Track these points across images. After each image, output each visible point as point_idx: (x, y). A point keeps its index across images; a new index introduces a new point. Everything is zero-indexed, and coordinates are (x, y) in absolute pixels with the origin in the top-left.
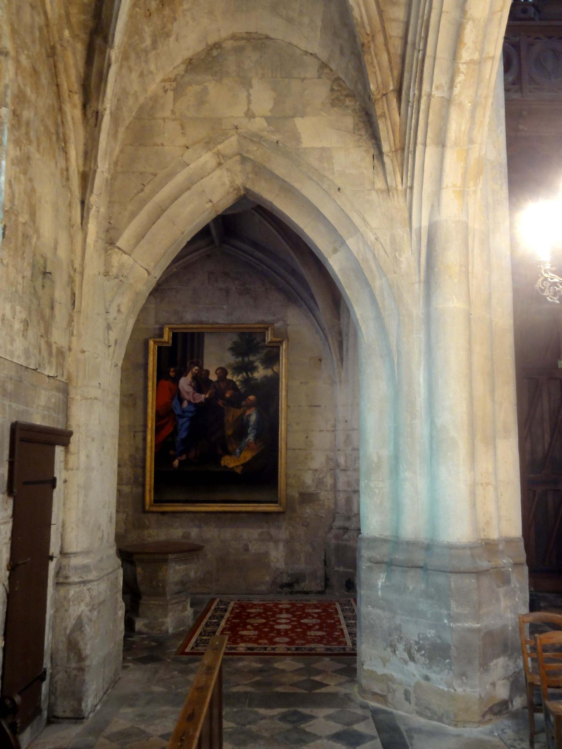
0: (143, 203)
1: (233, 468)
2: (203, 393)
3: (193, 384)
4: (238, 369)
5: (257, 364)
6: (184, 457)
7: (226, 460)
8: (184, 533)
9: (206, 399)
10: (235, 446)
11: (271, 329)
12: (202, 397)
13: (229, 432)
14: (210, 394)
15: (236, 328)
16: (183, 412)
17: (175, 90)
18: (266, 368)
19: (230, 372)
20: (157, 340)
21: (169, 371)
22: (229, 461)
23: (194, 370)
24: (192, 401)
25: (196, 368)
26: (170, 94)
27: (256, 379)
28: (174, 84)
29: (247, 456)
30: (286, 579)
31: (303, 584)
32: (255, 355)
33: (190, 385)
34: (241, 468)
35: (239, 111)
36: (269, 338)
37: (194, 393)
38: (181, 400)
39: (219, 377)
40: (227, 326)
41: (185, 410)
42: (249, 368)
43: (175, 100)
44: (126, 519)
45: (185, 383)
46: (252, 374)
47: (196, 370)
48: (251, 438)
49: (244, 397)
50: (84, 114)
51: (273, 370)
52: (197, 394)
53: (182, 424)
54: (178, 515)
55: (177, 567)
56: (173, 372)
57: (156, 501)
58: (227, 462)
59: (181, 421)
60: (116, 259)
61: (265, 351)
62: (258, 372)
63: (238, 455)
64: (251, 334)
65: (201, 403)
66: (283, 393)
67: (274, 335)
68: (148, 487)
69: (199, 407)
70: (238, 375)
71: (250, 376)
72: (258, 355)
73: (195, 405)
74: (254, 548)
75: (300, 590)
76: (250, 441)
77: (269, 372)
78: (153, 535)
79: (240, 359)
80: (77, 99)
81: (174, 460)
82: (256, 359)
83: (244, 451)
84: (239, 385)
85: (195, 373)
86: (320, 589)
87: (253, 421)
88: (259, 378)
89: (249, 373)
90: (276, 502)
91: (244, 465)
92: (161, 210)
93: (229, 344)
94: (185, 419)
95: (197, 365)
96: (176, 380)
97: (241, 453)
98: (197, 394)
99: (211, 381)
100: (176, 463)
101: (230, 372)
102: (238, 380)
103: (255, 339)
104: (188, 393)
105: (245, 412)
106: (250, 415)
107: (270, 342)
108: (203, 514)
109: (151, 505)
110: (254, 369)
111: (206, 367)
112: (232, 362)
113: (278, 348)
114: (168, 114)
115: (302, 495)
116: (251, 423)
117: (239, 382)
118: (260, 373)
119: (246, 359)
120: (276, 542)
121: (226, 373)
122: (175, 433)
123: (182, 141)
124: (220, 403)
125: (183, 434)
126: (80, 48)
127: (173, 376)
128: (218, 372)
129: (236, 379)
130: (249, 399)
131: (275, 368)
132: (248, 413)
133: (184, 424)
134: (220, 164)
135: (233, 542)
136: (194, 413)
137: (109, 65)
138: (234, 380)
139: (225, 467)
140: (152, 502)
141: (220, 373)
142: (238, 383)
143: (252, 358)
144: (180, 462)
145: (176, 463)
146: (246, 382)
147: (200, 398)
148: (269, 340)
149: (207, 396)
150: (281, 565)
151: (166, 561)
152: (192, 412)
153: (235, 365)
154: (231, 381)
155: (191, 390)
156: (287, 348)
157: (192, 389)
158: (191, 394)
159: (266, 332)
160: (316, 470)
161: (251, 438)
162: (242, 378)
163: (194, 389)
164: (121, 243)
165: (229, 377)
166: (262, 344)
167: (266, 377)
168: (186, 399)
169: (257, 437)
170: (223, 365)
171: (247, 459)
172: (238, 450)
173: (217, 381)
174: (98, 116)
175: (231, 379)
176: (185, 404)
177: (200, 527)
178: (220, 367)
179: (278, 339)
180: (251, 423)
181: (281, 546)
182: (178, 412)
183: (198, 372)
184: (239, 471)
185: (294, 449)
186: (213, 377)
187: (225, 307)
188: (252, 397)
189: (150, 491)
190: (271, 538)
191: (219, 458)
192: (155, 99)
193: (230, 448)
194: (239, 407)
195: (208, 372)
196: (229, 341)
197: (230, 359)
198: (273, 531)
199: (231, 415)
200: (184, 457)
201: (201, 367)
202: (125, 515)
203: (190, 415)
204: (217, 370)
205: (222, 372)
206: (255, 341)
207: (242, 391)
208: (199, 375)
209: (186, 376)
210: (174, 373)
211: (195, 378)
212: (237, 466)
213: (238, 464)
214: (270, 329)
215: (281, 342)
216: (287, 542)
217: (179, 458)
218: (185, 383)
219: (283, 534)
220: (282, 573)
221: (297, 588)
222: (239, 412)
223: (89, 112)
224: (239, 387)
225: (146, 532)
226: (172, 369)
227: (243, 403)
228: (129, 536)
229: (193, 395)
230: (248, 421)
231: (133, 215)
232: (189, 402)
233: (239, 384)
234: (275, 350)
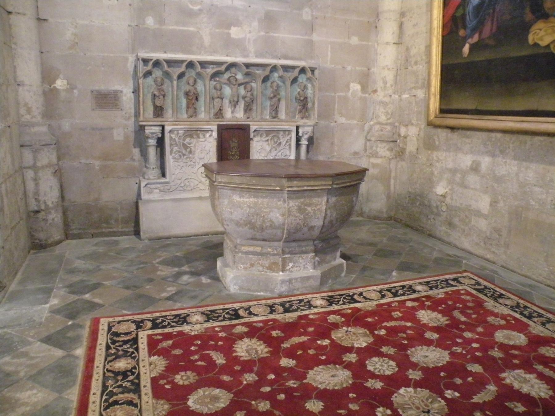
6: (476, 38)
8: (473, 162)
44: (418, 135)
54: (469, 133)
55: (236, 198)
57: (442, 111)
68: (433, 89)
78: (441, 160)
100: (466, 49)
135: (537, 189)
140: (438, 113)
145: (466, 49)
177: (493, 156)
200: (476, 38)
202: (418, 129)
225: (435, 154)
228: (420, 157)
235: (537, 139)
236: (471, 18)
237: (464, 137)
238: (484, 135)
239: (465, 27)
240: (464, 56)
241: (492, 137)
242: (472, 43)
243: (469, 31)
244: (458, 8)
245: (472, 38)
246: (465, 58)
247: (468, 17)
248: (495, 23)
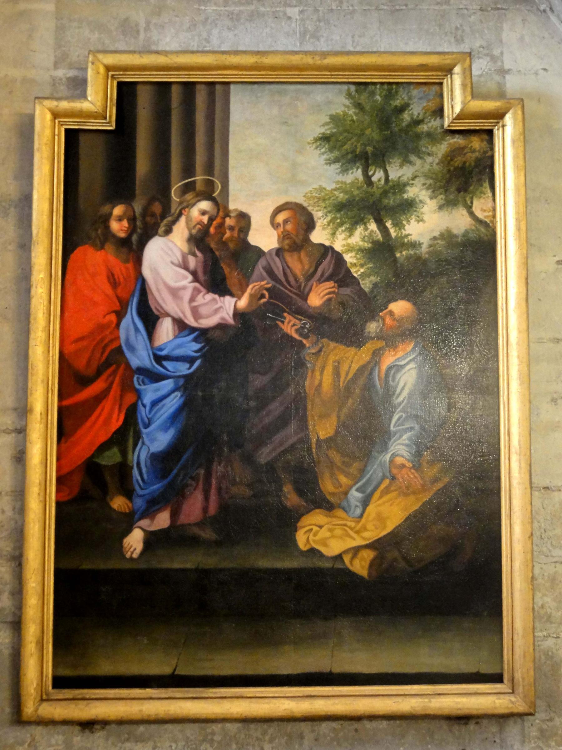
1: (339, 557)
2: (232, 295)
3: (192, 262)
7: (315, 528)
9: (237, 314)
10: (343, 480)
11: (464, 71)
14: (251, 296)
15: (343, 68)
16: (159, 359)
20: (64, 105)
21: (106, 219)
22: (324, 533)
23: (195, 212)
24: (191, 321)
25: (205, 205)
27: (414, 245)
32: (406, 161)
33: (185, 267)
34: (369, 555)
37: (196, 292)
39: (284, 237)
40: (309, 60)
41: (163, 353)
46: (398, 225)
47: (204, 213)
51: (472, 214)
53: (154, 403)
56: (120, 219)
58: (315, 535)
61: (442, 149)
62: (420, 220)
63: (358, 511)
65: (221, 327)
70: (351, 231)
71: (393, 232)
72: (418, 162)
76: (399, 460)
79: (357, 174)
81: (128, 531)
83: (377, 495)
84: (355, 265)
85: (200, 223)
87: (405, 393)
88: (425, 241)
89: (389, 224)
90: (498, 678)
94: (167, 385)
95: (208, 195)
97: (366, 503)
98: (210, 296)
99: (259, 252)
102: (350, 249)
104: (175, 292)
105: (377, 354)
106: (396, 368)
107: (460, 117)
108: (232, 728)
109: (44, 699)
112: (330, 186)
116: (401, 399)
117: (353, 254)
119: (378, 176)
121: (310, 225)
127: (122, 235)
128: (280, 218)
130: (391, 313)
132: (388, 360)
136: (197, 363)
138: (338, 247)
139: (313, 552)
141: (286, 222)
142: (349, 258)
147: (217, 311)
148: (457, 110)
149: (243, 303)
152: (191, 360)
153: (341, 196)
154: (326, 250)
157: (190, 278)
158: (187, 295)
159: (446, 82)
162: (363, 239)
163: (196, 279)
166: (433, 124)
168: (167, 315)
171: (390, 527)
172: (355, 495)
173: (279, 252)
175: (327, 243)
178: (287, 203)
179: (490, 105)
180: (401, 399)
183: (211, 220)
185: (546, 488)
187: (293, 12)
189: (41, 644)
203: (183, 369)
204: (278, 210)
206: (406, 117)
207: (366, 285)
208: (212, 230)
209: (168, 231)
210: (125, 223)
212: (356, 550)
213: (359, 542)
214: (457, 69)
215: (499, 116)
217: (144, 523)
224: (356, 272)
226: (118, 210)
227: (372, 327)
229: (192, 299)
230: (389, 393)
233: (354, 261)
234: (476, 143)
235: (325, 727)
236: (145, 476)
237: (128, 740)
239: (129, 494)
240: (128, 556)
241: (213, 733)
242: (152, 529)
243: (139, 503)
244: (104, 447)
245: (152, 518)
246: (131, 559)
247: (135, 471)
248: (213, 497)
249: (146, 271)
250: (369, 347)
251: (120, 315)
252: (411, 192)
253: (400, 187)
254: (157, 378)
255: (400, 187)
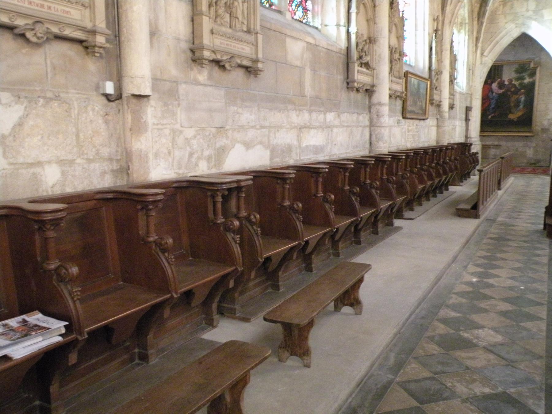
0: (493, 41)
1: (513, 119)
4: (517, 79)
5: (526, 77)
6: (493, 115)
9: (503, 92)
12: (501, 91)
13: (512, 104)
17: (503, 5)
18: (529, 78)
19: (514, 80)
25: (499, 79)
26: (502, 6)
28: (503, 3)
29: (519, 114)
30: (533, 162)
31: (540, 163)
35: (524, 9)
36: (532, 65)
38: (492, 92)
42: (523, 78)
43: (503, 7)
45: (494, 86)
48: (521, 107)
49: (520, 90)
50: (478, 22)
52: (499, 90)
53: (493, 102)
59: (492, 101)
60: (484, 59)
61: (530, 71)
64: (524, 64)
66: (536, 88)
67: (535, 64)
69: (500, 95)
73: (499, 94)
74: (520, 149)
75: (539, 165)
77: (531, 80)
79: (518, 75)
80: (476, 19)
82: (525, 75)
86: (547, 165)
91: (518, 118)
92: (497, 43)
93: (514, 69)
94: (494, 100)
95: (500, 78)
96: (491, 85)
100: (490, 117)
101: (514, 80)
103: (525, 66)
104: (496, 89)
105: (519, 96)
110: (524, 79)
111: (503, 79)
112: (515, 76)
113: (536, 69)
114: (500, 12)
115: (542, 129)
118: (527, 80)
120: (530, 148)
122: (490, 105)
123: (505, 21)
124: (509, 93)
125: (493, 106)
126: (478, 6)
129: (516, 83)
131: (534, 78)
132: (521, 97)
133: (493, 102)
134: (516, 27)
137: (487, 11)
142: (517, 85)
143: (524, 74)
144: (492, 117)
145: (490, 117)
146: (521, 84)
150: (531, 156)
151: (490, 148)
154: (514, 85)
155: (497, 88)
156: (540, 70)
160: (549, 119)
161: (521, 107)
164: (485, 54)
165: (513, 82)
167: (529, 82)
169: (524, 106)
170: (511, 78)
174: (482, 23)
176: (494, 94)
179: (536, 66)
181: (532, 149)
182: (491, 97)
184: (515, 120)
186: (506, 83)
188: (523, 91)
190: (528, 146)
191: (507, 115)
192: (497, 8)
193: (512, 111)
194: (517, 95)
195: (504, 81)
196: (514, 67)
197: (514, 75)
198: (529, 143)
199: (513, 98)
201: (501, 79)
203: (496, 98)
205: (510, 81)
211: (499, 83)
215: (537, 67)
216: (534, 148)
218: (494, 86)
219: (534, 145)
220: (531, 159)
221: (537, 165)
222: (517, 97)
223: (479, 21)
224: (518, 87)
226: (489, 80)
227: (519, 93)
231: (489, 45)
232: (496, 94)
238: (495, 137)
239: (489, 112)
249: (492, 87)
250: (519, 95)
251: (489, 92)
252: (526, 77)
253: (524, 76)
254: (493, 99)
255: (524, 76)
